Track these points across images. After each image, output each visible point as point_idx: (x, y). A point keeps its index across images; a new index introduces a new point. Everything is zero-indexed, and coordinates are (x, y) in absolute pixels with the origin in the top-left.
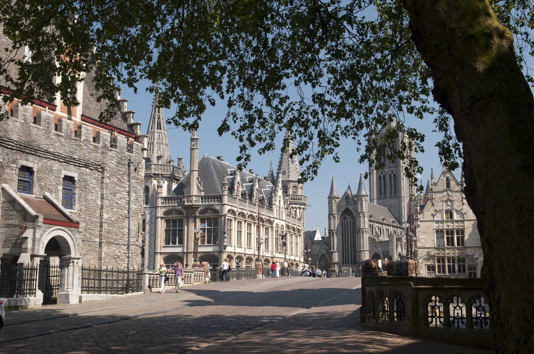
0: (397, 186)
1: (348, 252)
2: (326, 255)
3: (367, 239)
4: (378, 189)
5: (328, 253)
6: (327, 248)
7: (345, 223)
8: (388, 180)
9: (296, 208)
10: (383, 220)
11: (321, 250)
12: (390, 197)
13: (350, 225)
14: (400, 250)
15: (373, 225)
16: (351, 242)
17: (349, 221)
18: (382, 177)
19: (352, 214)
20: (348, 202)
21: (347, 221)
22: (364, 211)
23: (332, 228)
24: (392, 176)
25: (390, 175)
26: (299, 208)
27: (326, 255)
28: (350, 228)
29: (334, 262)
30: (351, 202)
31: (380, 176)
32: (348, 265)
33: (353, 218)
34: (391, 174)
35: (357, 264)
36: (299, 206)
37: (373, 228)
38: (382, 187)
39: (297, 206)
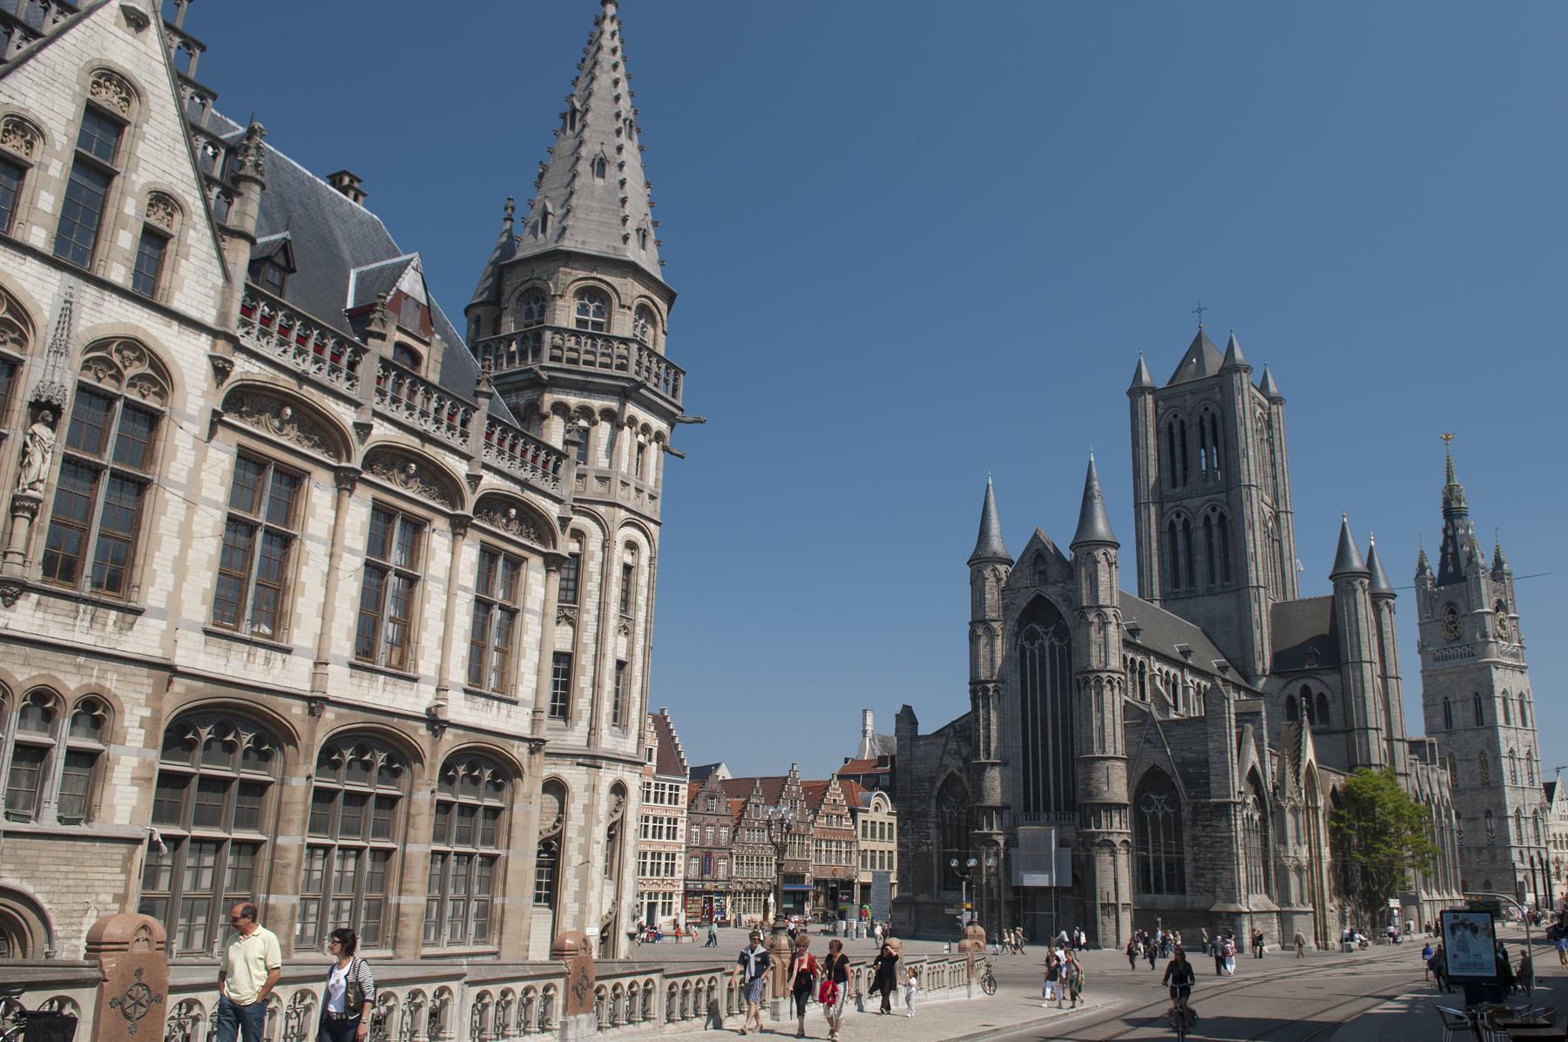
0: (1231, 553)
1: (1045, 765)
2: (964, 777)
3: (1118, 711)
4: (1168, 567)
5: (968, 771)
6: (965, 751)
7: (1033, 652)
8: (1199, 536)
9: (586, 412)
10: (1186, 653)
11: (945, 761)
12: (1210, 593)
13: (1053, 662)
14: (1253, 757)
15: (1142, 664)
16: (1055, 726)
17: (1047, 646)
18: (1179, 527)
19: (1060, 616)
20: (1042, 573)
21: (1042, 646)
22: (1101, 602)
23: (984, 673)
24: (1214, 520)
25: (1207, 519)
26: (608, 415)
27: (964, 777)
28: (1053, 672)
29: (990, 803)
30: (1054, 571)
31: (1172, 526)
32: (1043, 816)
33: (1063, 633)
34: (1210, 513)
35: (1077, 815)
36: (614, 405)
37: (1142, 675)
38: (1182, 560)
39: (597, 404)
